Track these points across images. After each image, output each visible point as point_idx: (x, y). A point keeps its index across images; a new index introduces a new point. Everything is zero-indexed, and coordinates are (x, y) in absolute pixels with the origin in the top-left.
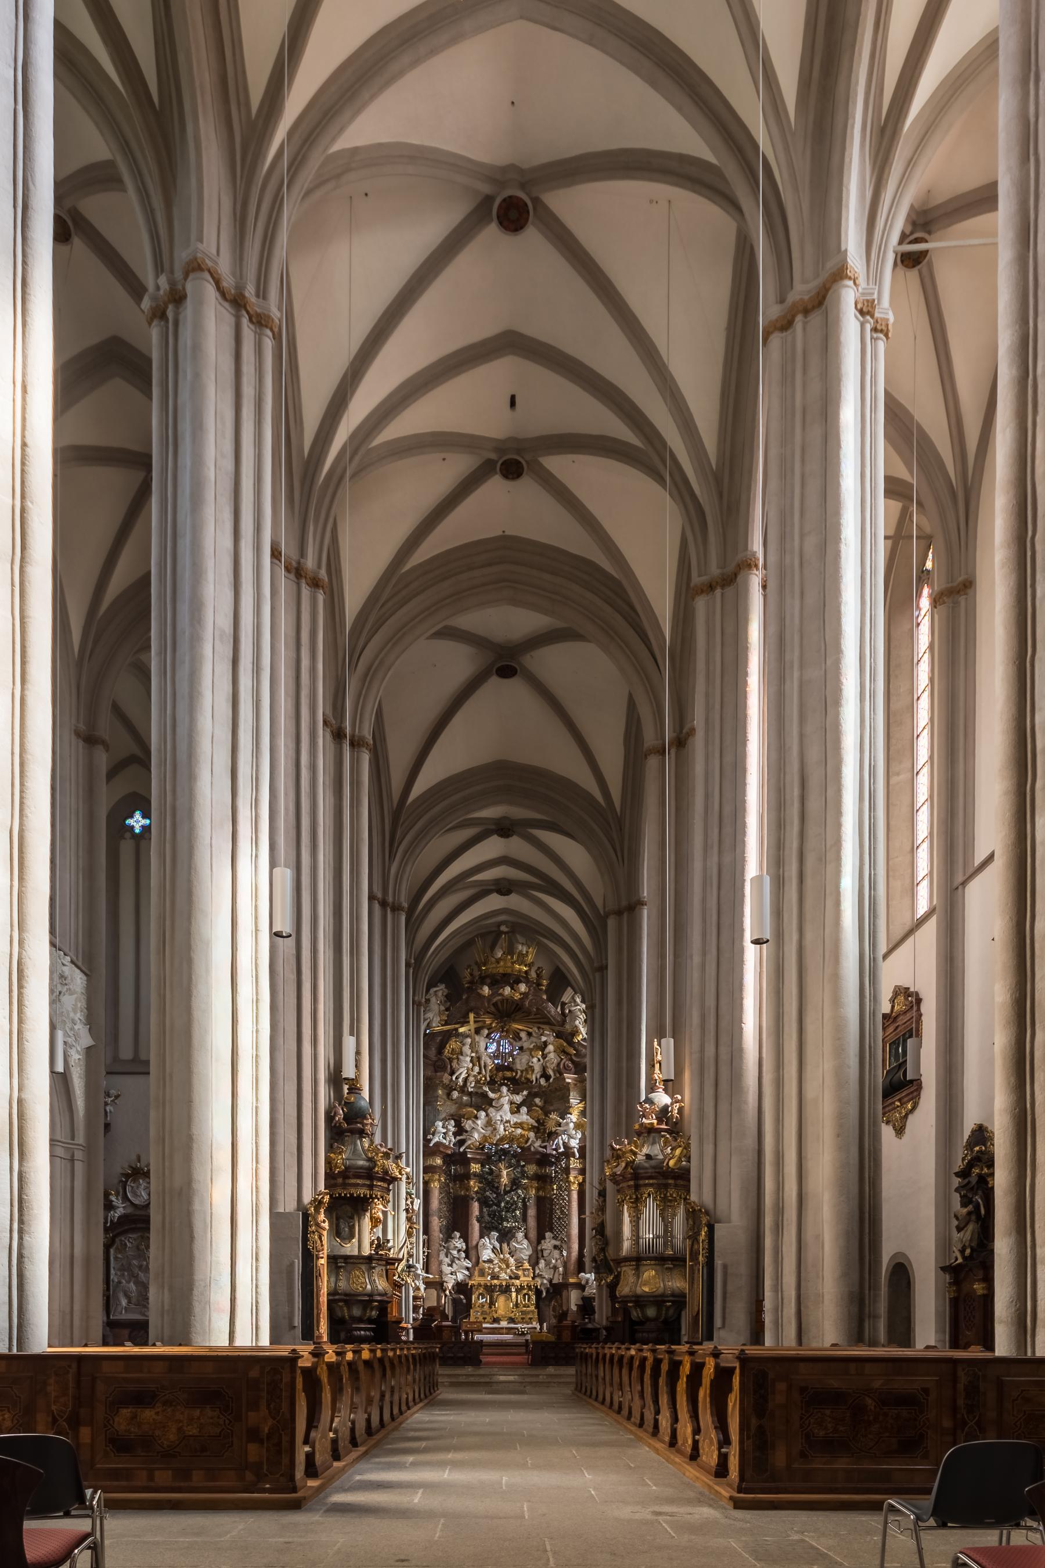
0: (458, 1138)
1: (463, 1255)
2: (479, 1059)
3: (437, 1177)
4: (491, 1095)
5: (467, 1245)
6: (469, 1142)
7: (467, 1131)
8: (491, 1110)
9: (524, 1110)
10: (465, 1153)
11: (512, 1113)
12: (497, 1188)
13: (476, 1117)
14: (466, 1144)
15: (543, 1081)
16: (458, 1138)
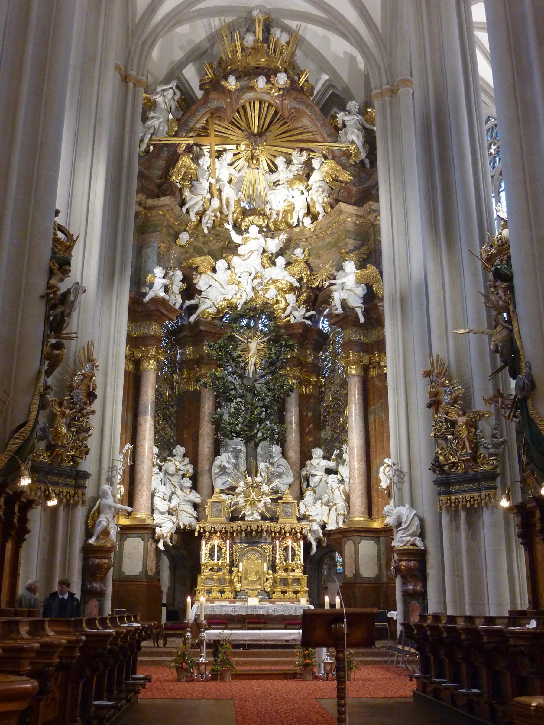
0: (188, 303)
1: (188, 483)
2: (220, 191)
3: (153, 351)
4: (236, 238)
5: (195, 469)
6: (202, 308)
7: (200, 292)
8: (235, 260)
9: (281, 261)
10: (197, 322)
11: (264, 266)
12: (244, 369)
13: (214, 270)
14: (199, 311)
15: (307, 221)
16: (188, 303)
